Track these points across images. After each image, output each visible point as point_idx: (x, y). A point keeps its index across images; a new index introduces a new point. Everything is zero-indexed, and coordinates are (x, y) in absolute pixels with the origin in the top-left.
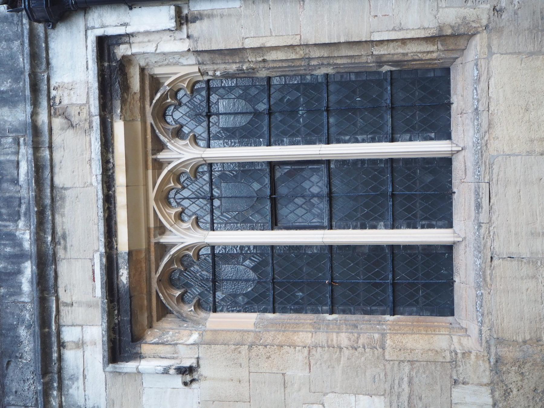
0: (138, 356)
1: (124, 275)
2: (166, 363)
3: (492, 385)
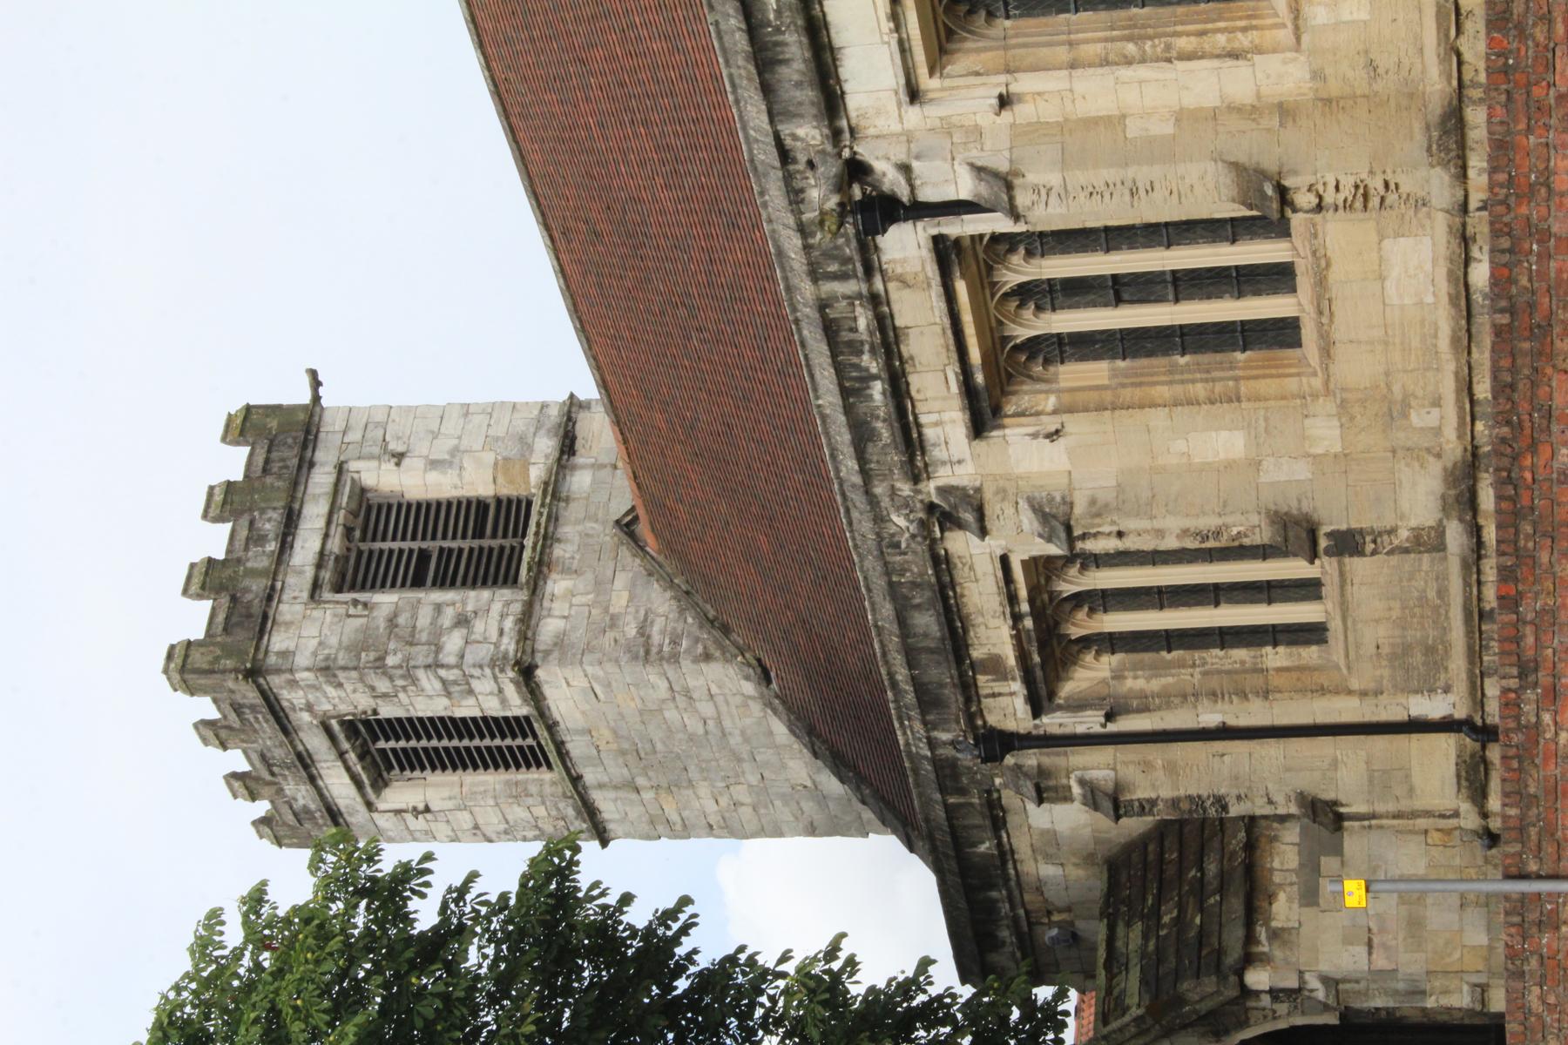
0: (1003, 427)
1: (979, 378)
2: (1031, 430)
3: (1339, 416)
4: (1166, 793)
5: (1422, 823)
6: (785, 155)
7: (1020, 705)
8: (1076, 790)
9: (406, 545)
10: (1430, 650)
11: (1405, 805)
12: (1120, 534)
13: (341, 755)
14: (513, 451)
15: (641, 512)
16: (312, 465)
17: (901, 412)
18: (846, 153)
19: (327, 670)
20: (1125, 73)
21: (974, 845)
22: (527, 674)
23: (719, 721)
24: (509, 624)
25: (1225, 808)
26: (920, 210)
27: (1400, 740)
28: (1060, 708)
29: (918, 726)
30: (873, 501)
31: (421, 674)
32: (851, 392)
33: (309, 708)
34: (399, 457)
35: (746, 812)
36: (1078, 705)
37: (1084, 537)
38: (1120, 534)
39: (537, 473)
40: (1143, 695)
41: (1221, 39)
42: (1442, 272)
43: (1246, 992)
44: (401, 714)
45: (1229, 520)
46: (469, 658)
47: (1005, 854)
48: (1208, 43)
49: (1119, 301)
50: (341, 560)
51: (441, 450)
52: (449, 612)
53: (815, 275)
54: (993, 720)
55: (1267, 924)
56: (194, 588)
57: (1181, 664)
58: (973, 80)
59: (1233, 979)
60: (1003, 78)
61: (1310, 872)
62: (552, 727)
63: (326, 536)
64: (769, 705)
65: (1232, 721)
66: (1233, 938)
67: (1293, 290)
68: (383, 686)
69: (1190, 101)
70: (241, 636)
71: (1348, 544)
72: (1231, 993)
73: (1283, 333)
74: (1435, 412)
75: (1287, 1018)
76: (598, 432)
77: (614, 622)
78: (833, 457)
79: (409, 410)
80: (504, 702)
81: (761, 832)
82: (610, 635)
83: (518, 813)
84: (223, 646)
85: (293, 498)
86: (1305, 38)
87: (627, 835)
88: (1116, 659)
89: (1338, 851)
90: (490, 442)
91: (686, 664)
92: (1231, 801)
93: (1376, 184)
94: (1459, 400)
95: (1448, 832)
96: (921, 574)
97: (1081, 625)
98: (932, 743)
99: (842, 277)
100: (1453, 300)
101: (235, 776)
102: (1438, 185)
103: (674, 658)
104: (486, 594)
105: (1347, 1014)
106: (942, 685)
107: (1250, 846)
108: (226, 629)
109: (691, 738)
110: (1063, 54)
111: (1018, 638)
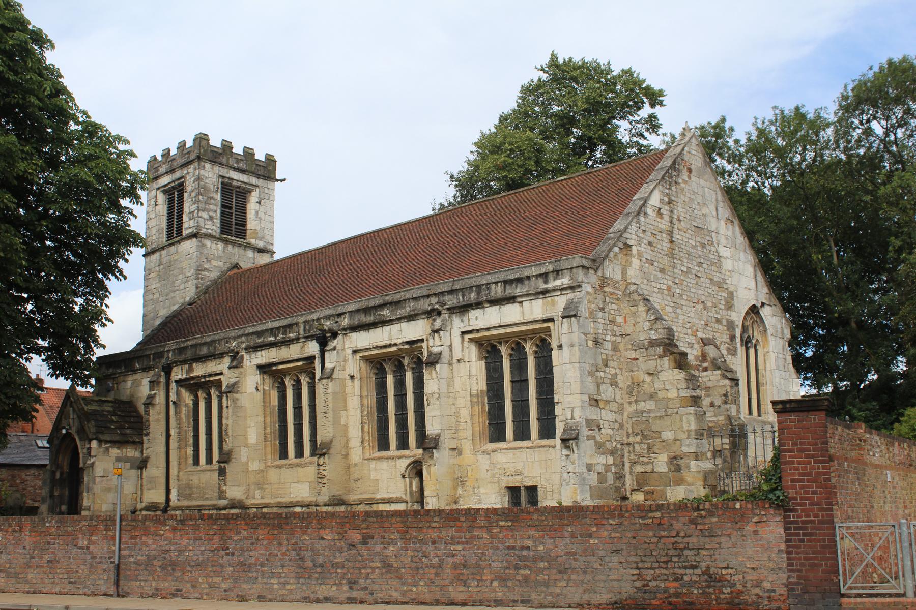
1: (274, 368)
3: (259, 470)
4: (151, 418)
5: (139, 492)
6: (340, 315)
7: (179, 377)
8: (153, 392)
9: (234, 203)
10: (190, 495)
11: (145, 487)
12: (227, 407)
13: (173, 181)
14: (260, 235)
15: (240, 270)
16: (258, 178)
17: (265, 345)
18: (340, 332)
19: (199, 179)
20: (359, 411)
21: (138, 363)
22: (194, 236)
23: (178, 290)
24: (210, 231)
25: (146, 435)
26: (322, 353)
27: (164, 486)
28: (177, 388)
29: (174, 347)
30: (240, 336)
31: (196, 205)
32: (272, 331)
33: (188, 173)
34: (259, 203)
35: (151, 297)
36: (178, 394)
37: (227, 397)
38: (227, 407)
39: (253, 241)
40: (180, 412)
41: (367, 438)
42: (299, 499)
43: (90, 441)
44: (185, 199)
45: (230, 438)
46: (200, 219)
47: (135, 371)
48: (366, 434)
49: (295, 408)
50: (231, 185)
51: (261, 214)
52: (214, 214)
53: (305, 322)
54: (175, 369)
55: (111, 447)
56: (224, 143)
57: (189, 424)
58: (358, 368)
59: (94, 437)
60: (359, 377)
61: (126, 460)
62: (179, 242)
63: (237, 181)
64: (182, 304)
65: (171, 438)
66: (107, 437)
67: (296, 457)
68: (193, 194)
69: (350, 429)
70: (210, 155)
71: (222, 472)
72: (90, 436)
73: (284, 454)
74: (259, 497)
75: (82, 452)
76: (264, 259)
77: (209, 261)
78: (253, 326)
79: (273, 206)
80: (187, 229)
81: (145, 301)
82: (205, 260)
83: (154, 231)
84: (207, 150)
85: (249, 172)
86: (366, 461)
87: (146, 262)
88: (191, 405)
89: (132, 468)
90: (263, 229)
91: (196, 281)
92: (148, 437)
93: (325, 481)
94: (262, 504)
95: (136, 500)
96: (218, 350)
97: (202, 395)
98: (168, 351)
99: (305, 330)
100: (291, 502)
101: (169, 151)
102: (323, 498)
103: (197, 278)
104: (219, 225)
105: (82, 470)
106: (186, 354)
107: (134, 443)
108: (212, 151)
109: (174, 282)
110: (365, 394)
111: (198, 377)
